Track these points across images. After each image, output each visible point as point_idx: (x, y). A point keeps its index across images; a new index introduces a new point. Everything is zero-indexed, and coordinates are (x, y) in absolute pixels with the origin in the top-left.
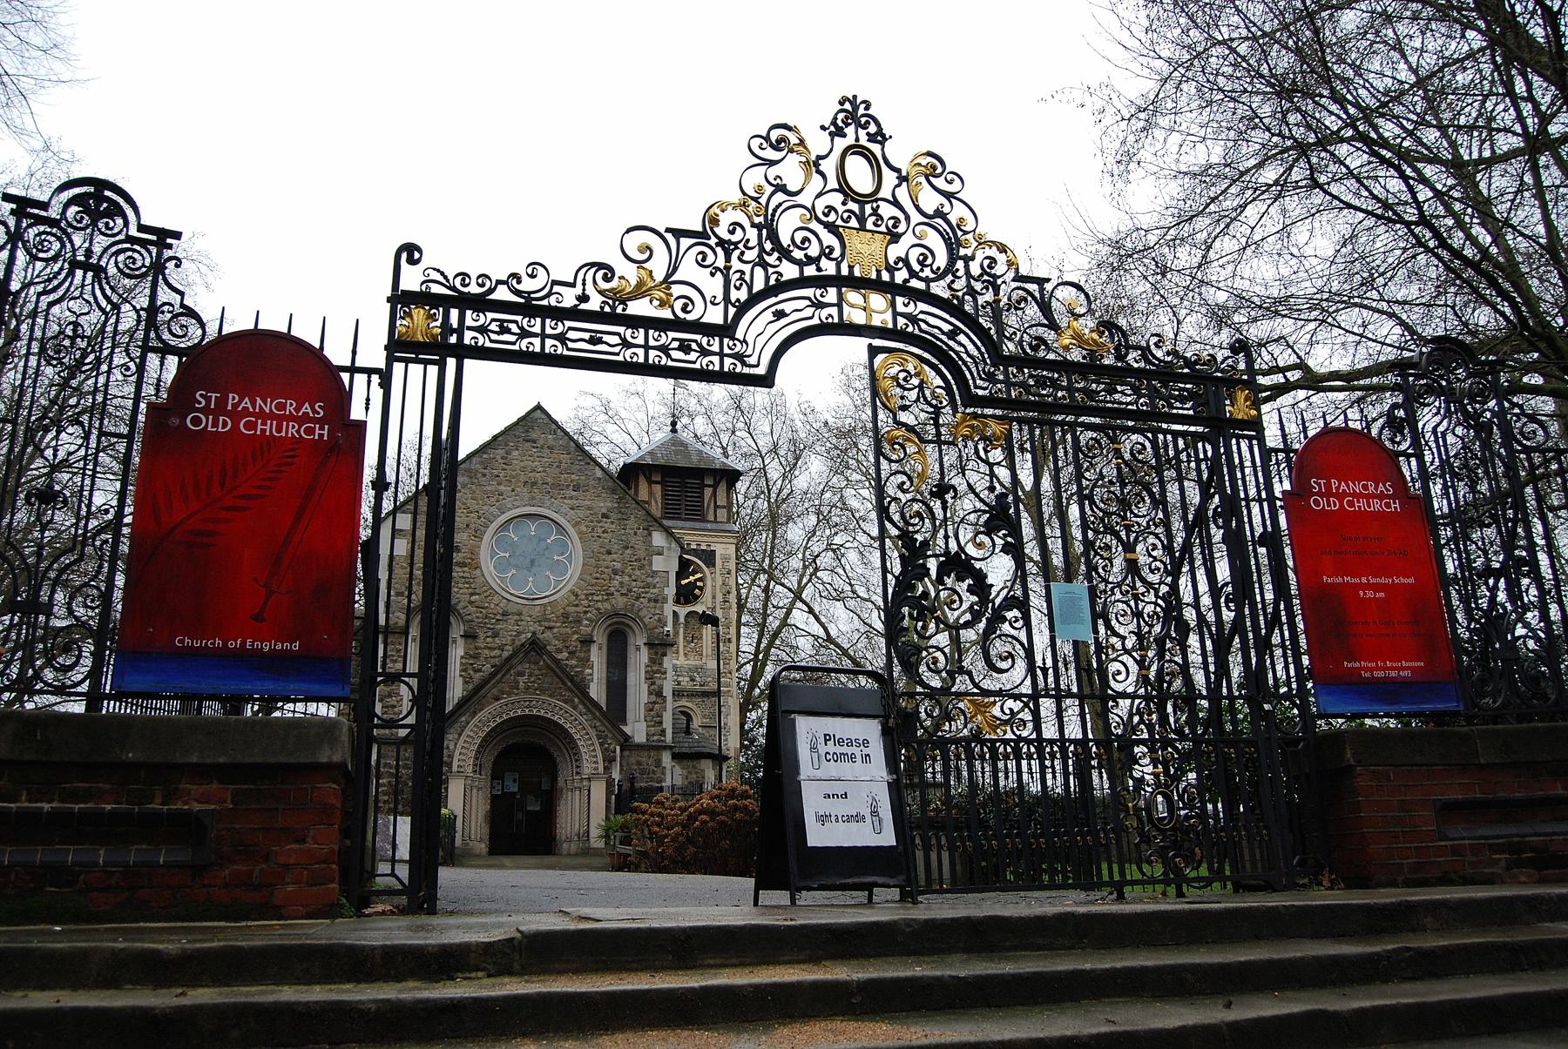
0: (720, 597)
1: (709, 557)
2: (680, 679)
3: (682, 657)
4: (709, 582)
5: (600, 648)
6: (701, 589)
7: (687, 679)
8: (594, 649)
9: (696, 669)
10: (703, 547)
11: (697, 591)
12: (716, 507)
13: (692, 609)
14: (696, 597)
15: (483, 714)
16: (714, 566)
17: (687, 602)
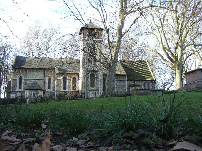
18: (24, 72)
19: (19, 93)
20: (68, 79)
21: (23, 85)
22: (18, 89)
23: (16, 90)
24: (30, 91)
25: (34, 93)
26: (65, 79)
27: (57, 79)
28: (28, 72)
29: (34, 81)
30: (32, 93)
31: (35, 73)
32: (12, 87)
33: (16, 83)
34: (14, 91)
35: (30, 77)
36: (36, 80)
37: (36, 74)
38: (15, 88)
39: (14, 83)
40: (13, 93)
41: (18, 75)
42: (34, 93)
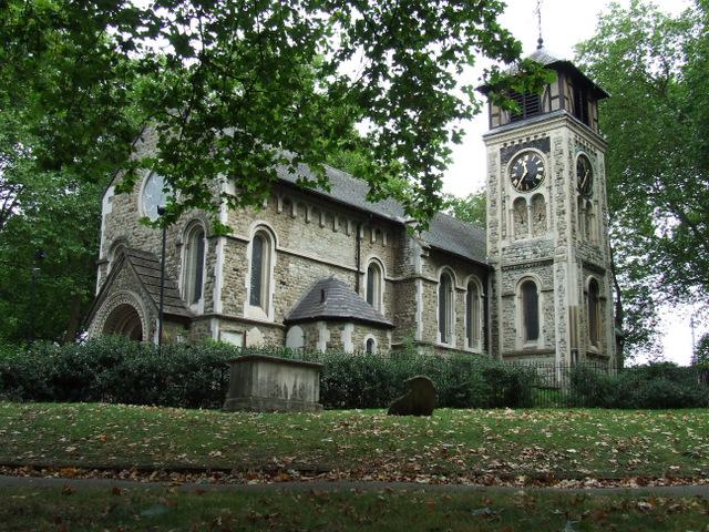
0: (554, 176)
1: (544, 145)
2: (526, 253)
3: (530, 236)
4: (546, 166)
5: (188, 247)
6: (541, 173)
7: (531, 253)
8: (183, 249)
9: (537, 244)
10: (540, 137)
11: (538, 177)
12: (551, 99)
13: (536, 192)
14: (538, 181)
15: (103, 308)
16: (549, 150)
17: (532, 187)
18: (280, 209)
19: (255, 330)
20: (459, 290)
21: (271, 286)
22: (250, 312)
23: (241, 312)
24: (355, 331)
25: (370, 342)
26: (445, 279)
27: (426, 280)
28: (295, 213)
29: (327, 272)
30: (365, 342)
31: (322, 227)
32: (225, 291)
33: (240, 266)
34: (231, 314)
35: (303, 243)
36: (323, 267)
37: (327, 231)
38: (235, 295)
39: (231, 266)
40: (231, 332)
41: (254, 217)
42: (370, 342)
